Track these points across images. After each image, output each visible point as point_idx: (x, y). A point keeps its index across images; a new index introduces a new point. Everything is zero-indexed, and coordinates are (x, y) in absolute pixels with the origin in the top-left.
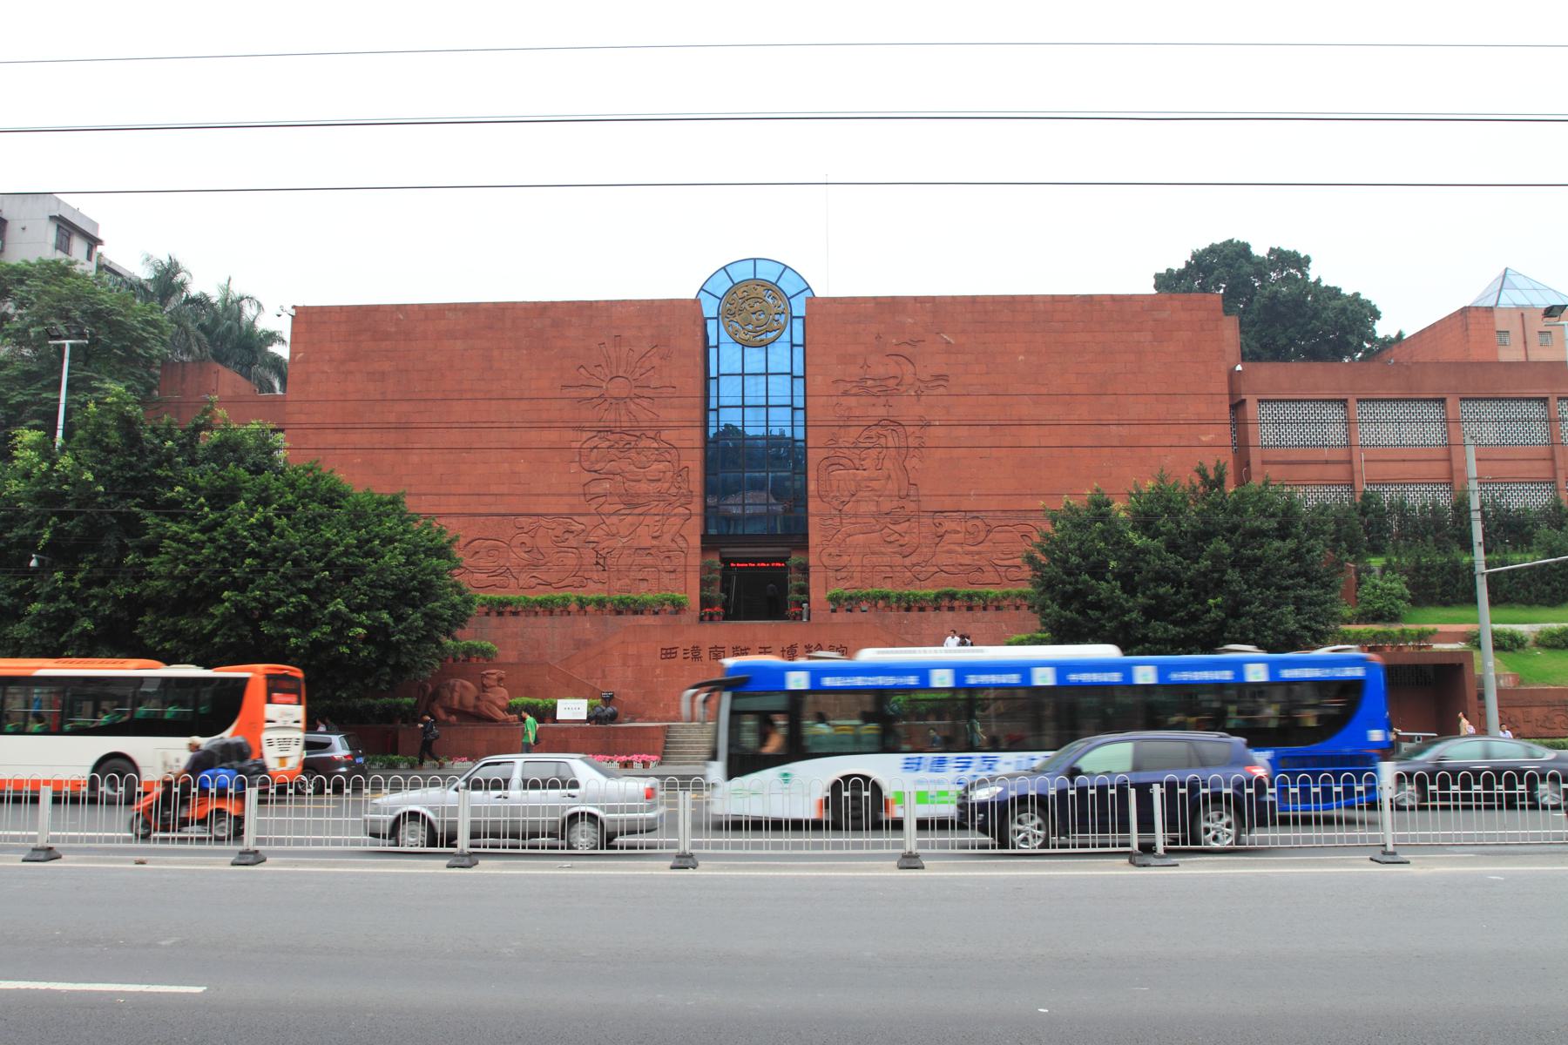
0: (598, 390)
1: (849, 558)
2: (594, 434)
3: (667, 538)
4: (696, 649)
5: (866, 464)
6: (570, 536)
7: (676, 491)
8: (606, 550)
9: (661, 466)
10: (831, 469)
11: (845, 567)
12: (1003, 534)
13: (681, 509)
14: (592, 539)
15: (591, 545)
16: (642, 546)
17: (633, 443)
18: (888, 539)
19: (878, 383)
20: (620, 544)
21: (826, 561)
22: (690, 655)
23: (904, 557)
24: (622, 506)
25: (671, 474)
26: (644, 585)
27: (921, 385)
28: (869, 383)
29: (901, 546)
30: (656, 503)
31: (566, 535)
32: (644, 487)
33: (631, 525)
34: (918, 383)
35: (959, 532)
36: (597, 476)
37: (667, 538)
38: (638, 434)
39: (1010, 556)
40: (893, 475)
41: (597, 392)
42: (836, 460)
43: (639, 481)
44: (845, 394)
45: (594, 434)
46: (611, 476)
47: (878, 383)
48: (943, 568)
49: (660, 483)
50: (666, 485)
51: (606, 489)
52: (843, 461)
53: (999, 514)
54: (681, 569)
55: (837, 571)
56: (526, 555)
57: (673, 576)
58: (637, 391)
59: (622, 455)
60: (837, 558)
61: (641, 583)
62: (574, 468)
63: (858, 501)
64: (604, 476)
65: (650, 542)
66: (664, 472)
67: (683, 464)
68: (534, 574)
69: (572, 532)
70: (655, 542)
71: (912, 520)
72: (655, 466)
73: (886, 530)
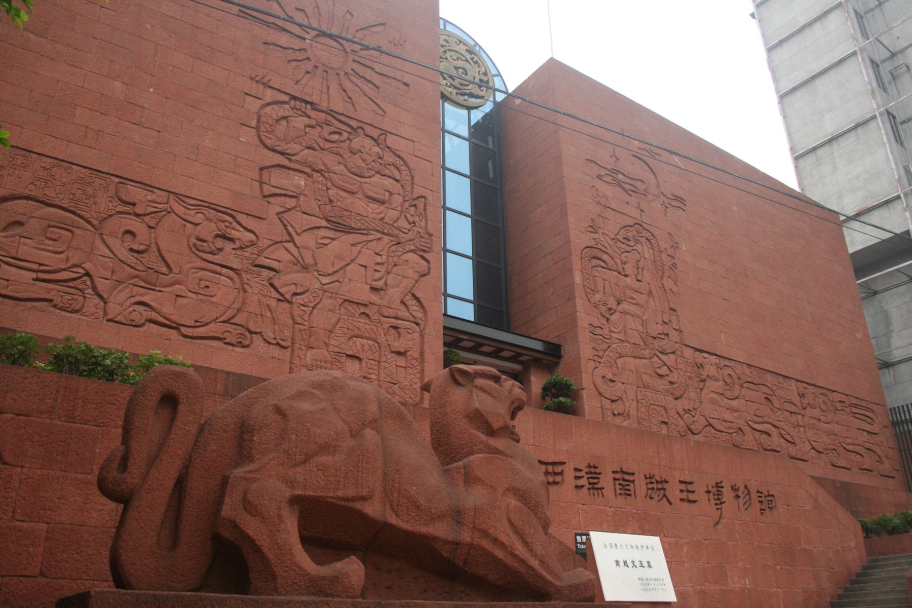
0: (298, 40)
2: (285, 98)
3: (394, 294)
4: (593, 473)
5: (629, 269)
6: (229, 246)
7: (408, 227)
8: (293, 289)
9: (388, 182)
10: (595, 262)
11: (620, 398)
12: (752, 392)
13: (412, 254)
14: (267, 262)
15: (265, 273)
16: (355, 298)
17: (345, 135)
18: (658, 371)
19: (627, 180)
20: (318, 285)
21: (599, 381)
23: (676, 399)
24: (324, 223)
25: (401, 200)
26: (353, 367)
27: (665, 199)
28: (620, 177)
29: (671, 383)
30: (380, 235)
31: (220, 243)
32: (360, 205)
33: (339, 257)
34: (661, 196)
35: (718, 380)
36: (286, 162)
37: (394, 294)
38: (354, 124)
39: (760, 420)
40: (654, 291)
41: (296, 44)
42: (600, 254)
43: (353, 193)
44: (599, 177)
45: (285, 98)
46: (308, 170)
47: (627, 180)
48: (711, 421)
49: (382, 208)
50: (395, 213)
51: (298, 186)
52: (605, 257)
53: (745, 366)
54: (414, 353)
55: (613, 401)
56: (131, 258)
57: (401, 361)
58: (356, 66)
59: (328, 145)
60: (611, 384)
62: (248, 136)
63: (624, 313)
64: (292, 165)
65: (362, 293)
66: (391, 194)
67: (418, 191)
68: (145, 299)
69: (232, 240)
70: (374, 298)
71: (678, 353)
72: (376, 179)
73: (655, 359)
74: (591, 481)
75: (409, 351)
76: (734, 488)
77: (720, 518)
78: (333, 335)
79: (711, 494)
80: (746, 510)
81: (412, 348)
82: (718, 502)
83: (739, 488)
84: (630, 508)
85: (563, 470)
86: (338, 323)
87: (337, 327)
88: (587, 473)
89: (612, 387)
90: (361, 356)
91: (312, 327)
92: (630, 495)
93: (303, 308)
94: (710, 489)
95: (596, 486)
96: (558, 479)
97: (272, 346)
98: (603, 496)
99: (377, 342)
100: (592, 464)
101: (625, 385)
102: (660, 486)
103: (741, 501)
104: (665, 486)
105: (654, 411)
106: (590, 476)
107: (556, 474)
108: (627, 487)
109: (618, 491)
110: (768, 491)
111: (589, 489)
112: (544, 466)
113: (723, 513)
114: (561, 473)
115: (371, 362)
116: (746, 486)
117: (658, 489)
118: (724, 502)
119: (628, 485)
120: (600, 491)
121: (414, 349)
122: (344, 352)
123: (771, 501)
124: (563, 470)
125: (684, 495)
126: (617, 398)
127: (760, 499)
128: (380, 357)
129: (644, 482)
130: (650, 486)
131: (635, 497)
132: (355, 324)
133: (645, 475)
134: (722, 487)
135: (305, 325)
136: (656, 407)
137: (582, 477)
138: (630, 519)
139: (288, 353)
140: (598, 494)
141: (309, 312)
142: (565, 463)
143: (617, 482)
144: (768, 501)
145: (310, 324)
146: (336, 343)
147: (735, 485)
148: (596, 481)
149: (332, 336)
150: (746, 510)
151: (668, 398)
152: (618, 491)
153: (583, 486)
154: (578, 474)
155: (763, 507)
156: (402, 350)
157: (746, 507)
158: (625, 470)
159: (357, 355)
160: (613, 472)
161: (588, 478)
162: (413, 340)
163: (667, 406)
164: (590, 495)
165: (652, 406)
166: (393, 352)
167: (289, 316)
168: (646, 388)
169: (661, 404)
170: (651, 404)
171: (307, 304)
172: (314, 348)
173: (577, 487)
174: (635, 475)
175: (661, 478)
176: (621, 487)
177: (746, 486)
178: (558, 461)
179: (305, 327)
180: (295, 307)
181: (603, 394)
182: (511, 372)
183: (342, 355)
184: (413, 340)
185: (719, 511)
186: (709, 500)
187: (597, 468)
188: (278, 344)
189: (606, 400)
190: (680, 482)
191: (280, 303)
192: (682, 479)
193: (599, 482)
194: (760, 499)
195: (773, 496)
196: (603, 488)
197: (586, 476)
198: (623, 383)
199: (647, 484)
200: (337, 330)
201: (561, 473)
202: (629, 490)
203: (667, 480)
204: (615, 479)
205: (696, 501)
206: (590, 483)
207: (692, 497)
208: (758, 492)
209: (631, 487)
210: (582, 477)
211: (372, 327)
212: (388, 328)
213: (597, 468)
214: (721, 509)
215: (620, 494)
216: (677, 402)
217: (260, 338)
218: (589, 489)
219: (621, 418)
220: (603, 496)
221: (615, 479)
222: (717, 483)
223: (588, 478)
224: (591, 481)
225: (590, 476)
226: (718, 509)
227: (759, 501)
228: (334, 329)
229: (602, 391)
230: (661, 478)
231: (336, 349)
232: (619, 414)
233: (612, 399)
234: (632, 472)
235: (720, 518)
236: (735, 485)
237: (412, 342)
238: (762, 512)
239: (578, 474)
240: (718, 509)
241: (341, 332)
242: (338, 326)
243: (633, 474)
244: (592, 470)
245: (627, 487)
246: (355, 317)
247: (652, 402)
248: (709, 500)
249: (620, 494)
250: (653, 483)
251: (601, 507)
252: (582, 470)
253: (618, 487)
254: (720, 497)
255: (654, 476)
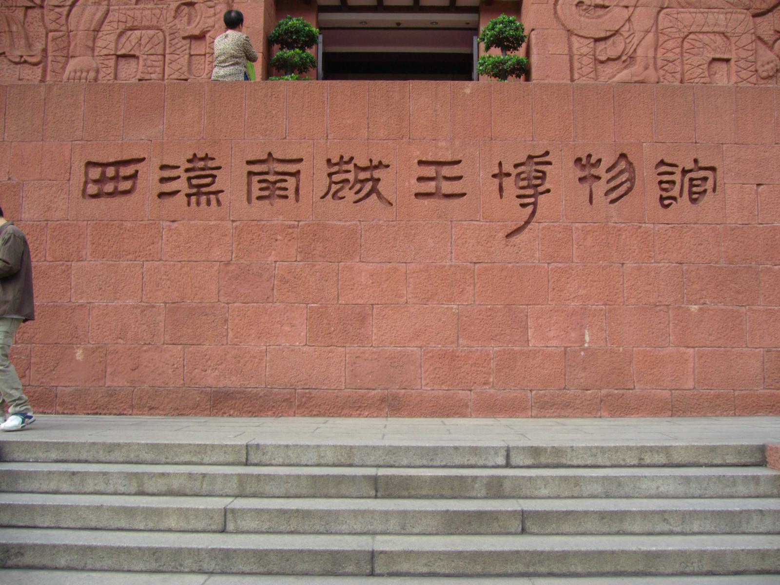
1: (626, 13)
11: (616, 33)
22: (181, 185)
23: (755, 16)
55: (597, 40)
60: (600, 12)
61: (123, 63)
74: (194, 182)
75: (209, 31)
76: (584, 162)
77: (527, 222)
78: (100, 34)
79: (508, 183)
80: (613, 202)
81: (214, 26)
82: (530, 192)
83: (599, 161)
84: (281, 217)
85: (137, 172)
86: (105, 18)
87: (105, 23)
88: (187, 170)
89: (599, 17)
90: (137, 54)
91: (71, 31)
92: (286, 197)
93: (57, 10)
94: (508, 168)
95: (204, 190)
96: (125, 185)
97: (19, 66)
98: (219, 203)
99: (161, 30)
100: (201, 155)
101: (631, 9)
102: (363, 176)
103: (599, 188)
104: (377, 174)
105: (697, 44)
106: (192, 174)
107: (126, 178)
108: (282, 185)
109: (256, 193)
110: (696, 161)
111: (189, 196)
112: (100, 169)
113: (538, 211)
114: (134, 176)
115: (153, 58)
116: (623, 156)
117: (357, 181)
118: (548, 191)
119: (285, 181)
120: (213, 197)
121: (216, 26)
122: (113, 52)
123: (705, 179)
124: (137, 172)
125: (431, 186)
126: (609, 34)
127: (665, 178)
128: (165, 50)
129: (325, 170)
130: (335, 178)
131: (297, 200)
132: (129, 13)
133: (329, 161)
134: (549, 163)
135: (61, 31)
136: (701, 36)
137: (179, 177)
138: (279, 237)
139: (39, 70)
140: (209, 203)
141: (65, 13)
142: (144, 159)
143: (256, 179)
144: (691, 180)
145: (68, 28)
146: (104, 44)
147: (589, 156)
148: (208, 180)
149: (99, 36)
150: (613, 202)
151: (734, 16)
152: (256, 193)
153: (175, 193)
154: (167, 174)
155: (675, 192)
156: (197, 32)
157: (614, 195)
158: (277, 155)
159: (132, 53)
160: (249, 163)
161: (189, 179)
162: (215, 15)
163: (729, 30)
164: (189, 204)
165: (691, 36)
166: (184, 38)
167: (41, 24)
168: (683, 7)
169: (716, 29)
170: (691, 33)
171: (62, 4)
172: (75, 57)
173: (161, 195)
174: (304, 163)
175: (371, 161)
176: (264, 185)
177: (623, 156)
178: (130, 158)
179: (61, 34)
180: (46, 11)
181: (575, 32)
182: (467, 26)
183: (109, 57)
184: (215, 15)
185: (530, 209)
186: (501, 189)
187: (213, 159)
188: (25, 62)
189: (582, 40)
190: (420, 163)
191: (30, 12)
192: (430, 158)
193: (213, 183)
194: (665, 178)
195: (713, 169)
196: (222, 191)
197: (184, 176)
198: (627, 7)
199: (330, 175)
200: (106, 27)
201: (134, 176)
202: (286, 189)
203: (385, 162)
204: (250, 174)
205: (464, 195)
206: (191, 186)
207: (447, 187)
208: (662, 163)
209: (291, 182)
210: (179, 177)
211: (154, 11)
212: (178, 7)
213: (213, 159)
214: (535, 204)
215: (259, 198)
216: (759, 20)
217: (6, 61)
218: (189, 196)
219: (618, 65)
220: (219, 203)
221: (250, 174)
222: (530, 157)
223: (189, 179)
224: (194, 182)
225: (192, 174)
226: (523, 205)
227: (661, 182)
228: (100, 28)
229: (570, 26)
230: (371, 161)
231: (105, 52)
232: (609, 59)
233: (597, 36)
234: (295, 157)
235: (527, 222)
236: (589, 156)
237: (213, 19)
238: (666, 202)
239: (167, 174)
240: (523, 205)
241: (109, 28)
242: (107, 20)
243: (300, 160)
244: (201, 164)
245: (278, 185)
246: (131, 4)
247: (693, 29)
248: (501, 189)
249: (259, 198)
250: (348, 171)
251: (212, 223)
252: (178, 167)
253: (256, 186)
254: (538, 182)
255: (352, 159)
